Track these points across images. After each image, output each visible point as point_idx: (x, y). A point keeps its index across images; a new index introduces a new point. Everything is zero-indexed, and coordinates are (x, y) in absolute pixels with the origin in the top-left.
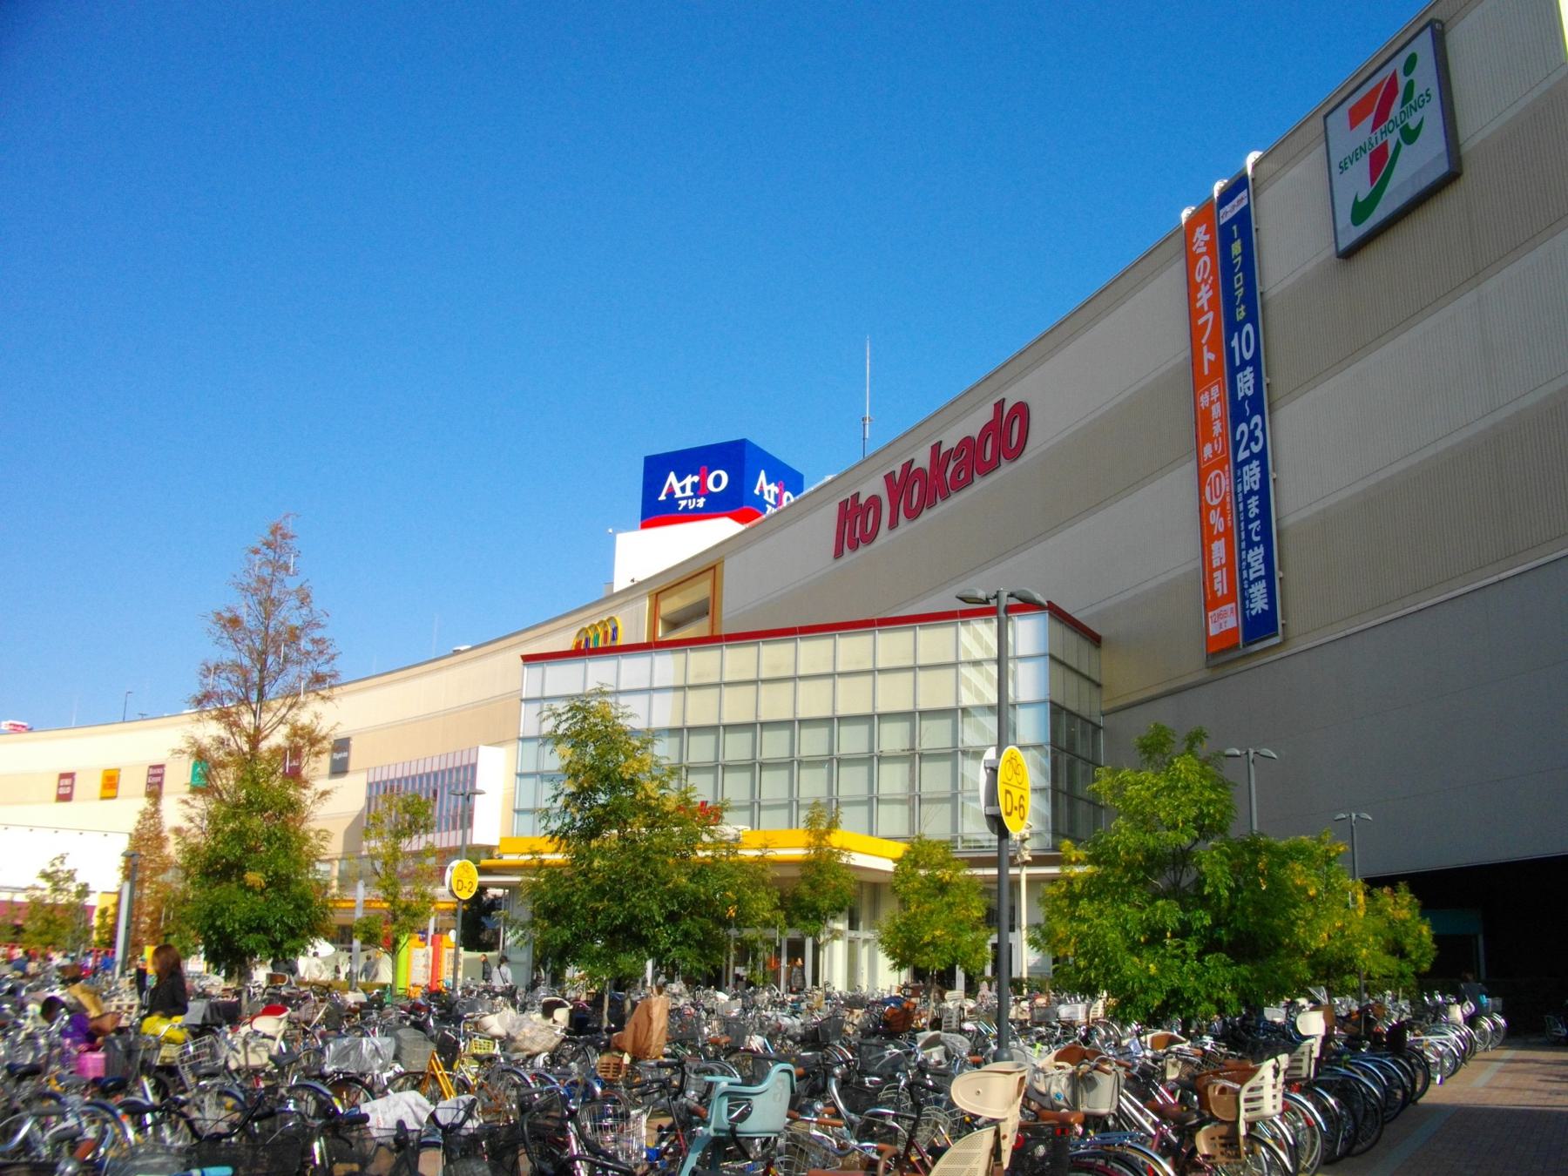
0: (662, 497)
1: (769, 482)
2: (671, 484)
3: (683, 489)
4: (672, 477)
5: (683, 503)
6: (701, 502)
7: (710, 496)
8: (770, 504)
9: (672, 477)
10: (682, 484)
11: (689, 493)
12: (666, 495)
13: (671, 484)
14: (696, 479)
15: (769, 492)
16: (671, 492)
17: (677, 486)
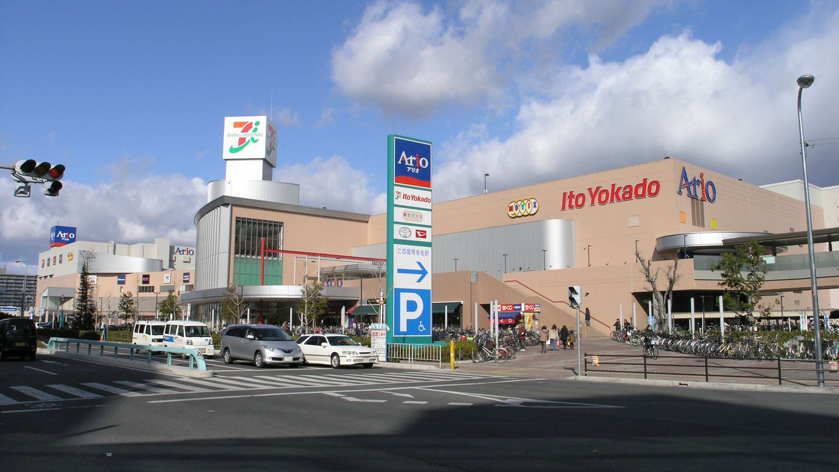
0: (400, 162)
1: (407, 157)
2: (403, 158)
3: (409, 161)
4: (404, 154)
5: (410, 168)
6: (418, 170)
7: (419, 167)
8: (410, 166)
9: (404, 154)
10: (408, 159)
11: (411, 164)
12: (401, 162)
13: (403, 158)
14: (415, 158)
15: (409, 161)
16: (403, 161)
17: (406, 160)
